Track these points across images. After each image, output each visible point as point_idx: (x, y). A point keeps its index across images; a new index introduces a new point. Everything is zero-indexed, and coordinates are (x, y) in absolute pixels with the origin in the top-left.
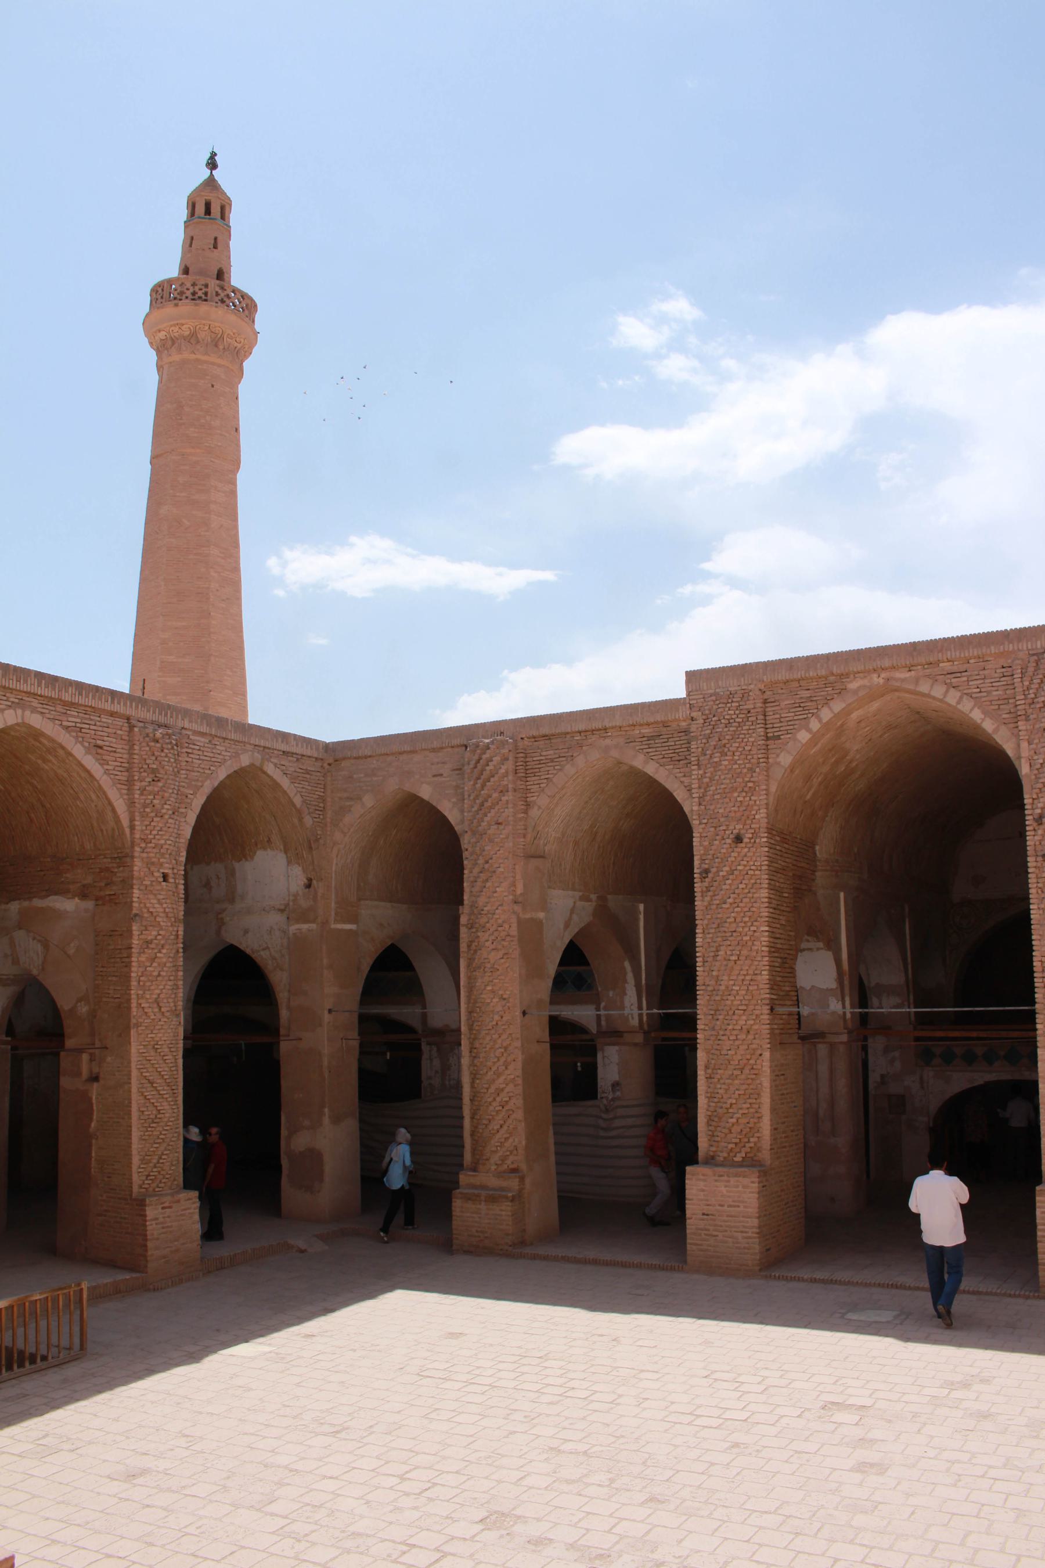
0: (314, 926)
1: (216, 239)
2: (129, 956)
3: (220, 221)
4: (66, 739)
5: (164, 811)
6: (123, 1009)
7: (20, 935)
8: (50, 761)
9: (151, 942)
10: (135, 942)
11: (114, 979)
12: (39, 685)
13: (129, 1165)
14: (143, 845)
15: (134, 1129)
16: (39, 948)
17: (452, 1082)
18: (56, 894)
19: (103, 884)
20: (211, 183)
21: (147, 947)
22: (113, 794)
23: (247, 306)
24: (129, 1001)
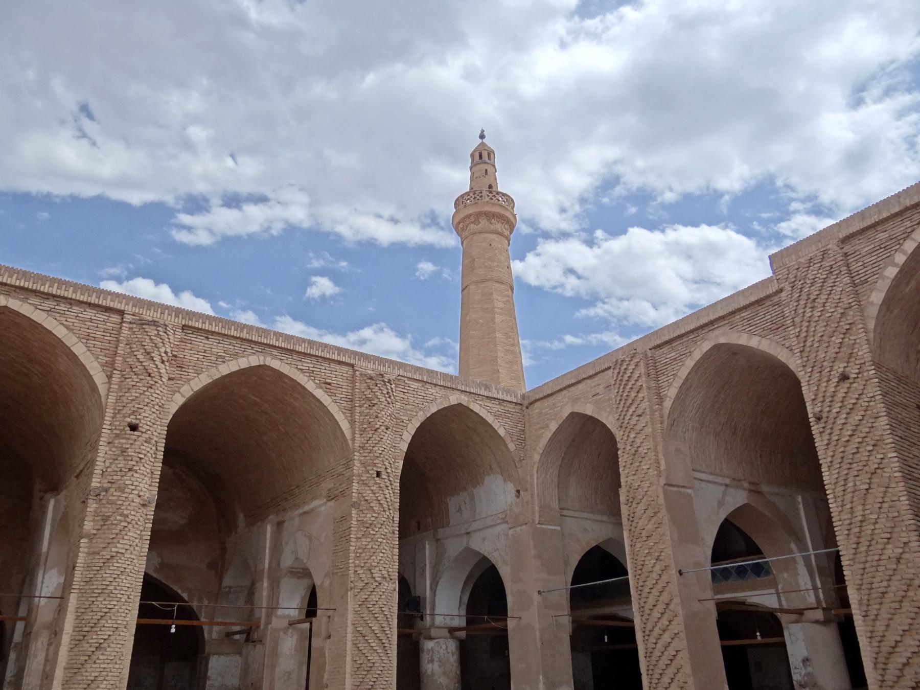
15: (348, 676)
16: (307, 542)
20: (482, 143)
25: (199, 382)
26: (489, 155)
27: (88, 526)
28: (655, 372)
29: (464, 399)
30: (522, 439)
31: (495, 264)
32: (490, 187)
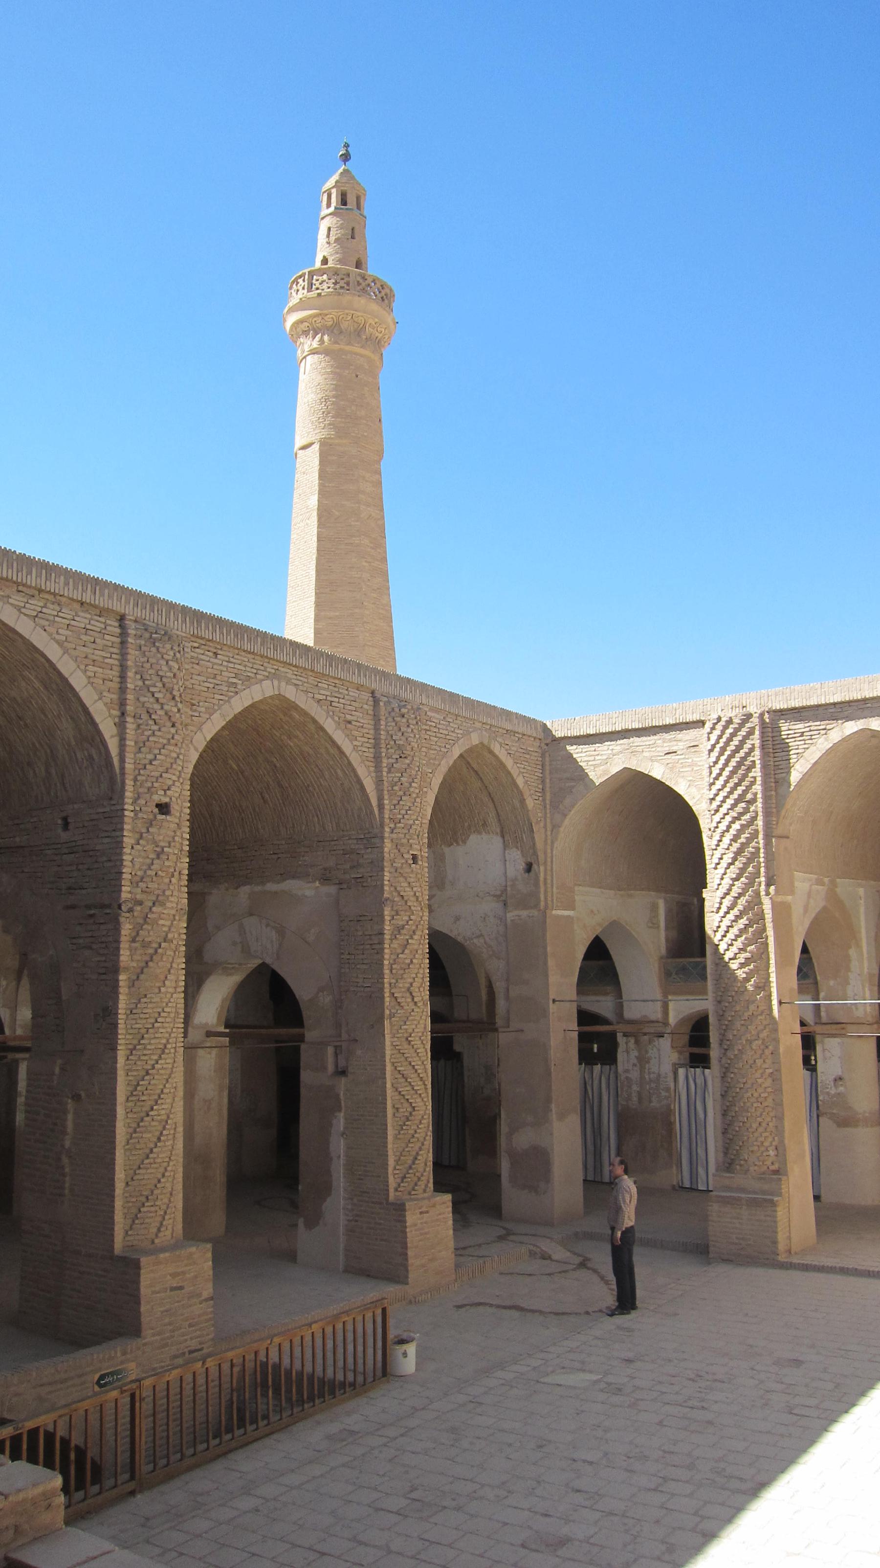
0: (535, 913)
1: (353, 229)
2: (381, 943)
3: (357, 212)
4: (319, 714)
5: (412, 790)
6: (375, 998)
7: (252, 924)
8: (296, 737)
9: (403, 927)
10: (387, 927)
11: (365, 967)
12: (294, 654)
13: (385, 1165)
14: (392, 826)
17: (652, 1076)
18: (293, 877)
19: (348, 866)
21: (399, 933)
22: (361, 771)
23: (385, 296)
24: (382, 990)
26: (358, 198)
31: (363, 413)
32: (358, 265)
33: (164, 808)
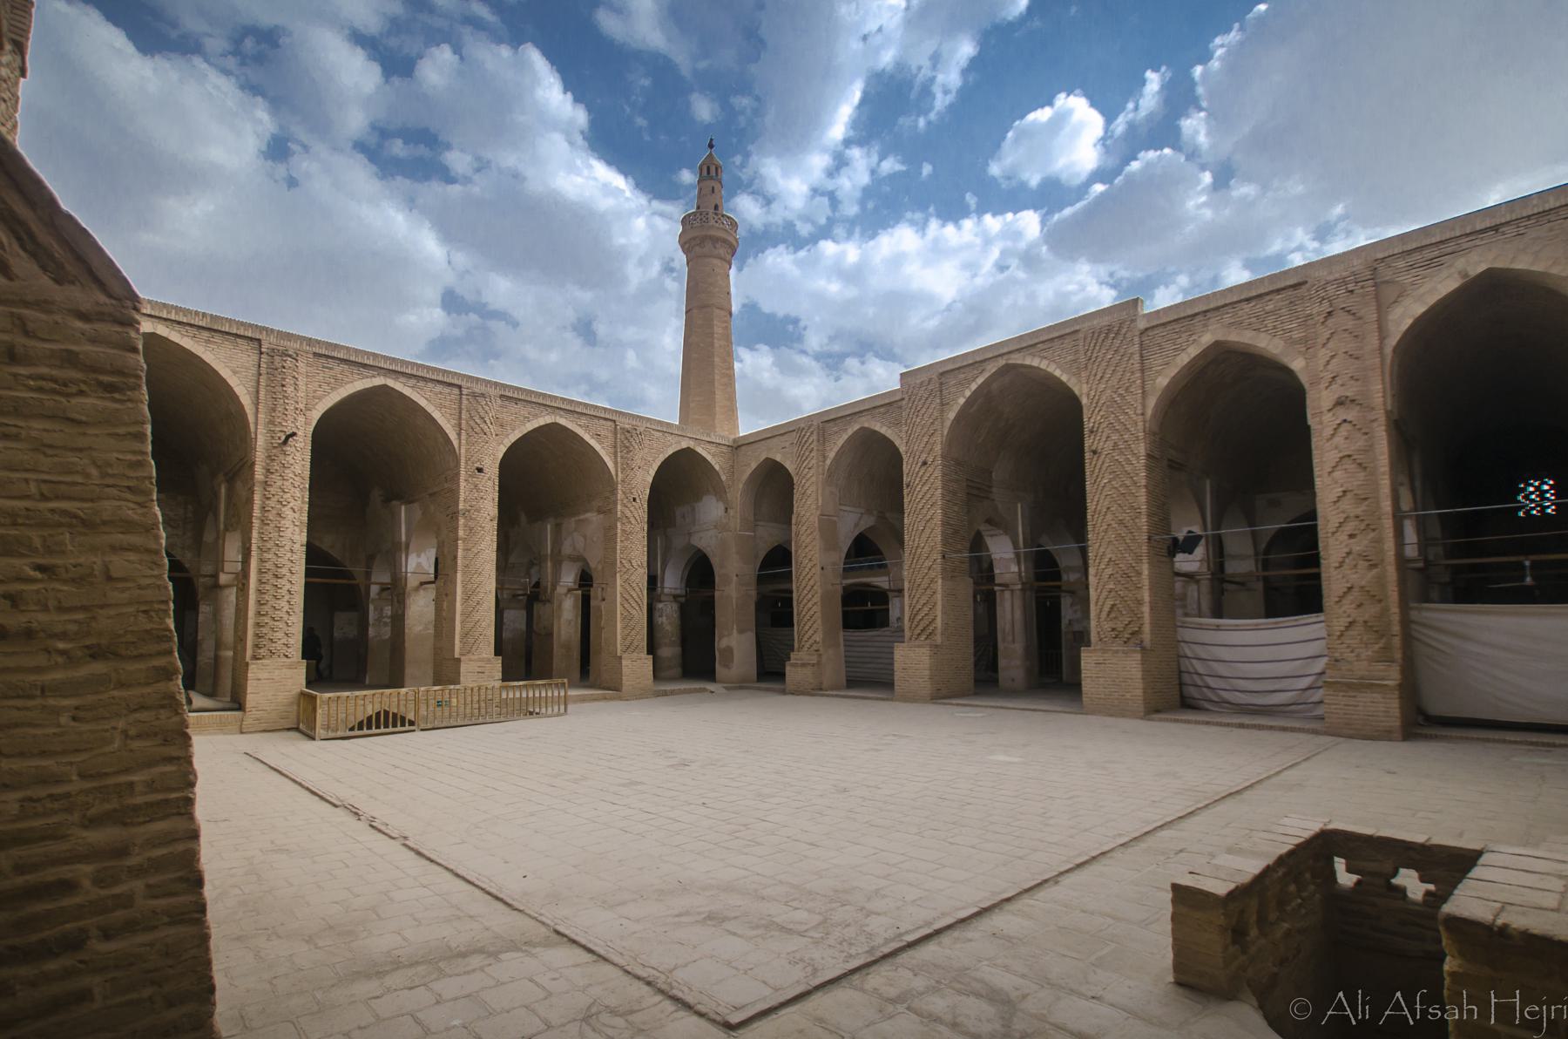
25: (515, 436)
27: (461, 533)
28: (823, 438)
29: (691, 444)
30: (732, 471)
32: (716, 207)
33: (480, 470)
